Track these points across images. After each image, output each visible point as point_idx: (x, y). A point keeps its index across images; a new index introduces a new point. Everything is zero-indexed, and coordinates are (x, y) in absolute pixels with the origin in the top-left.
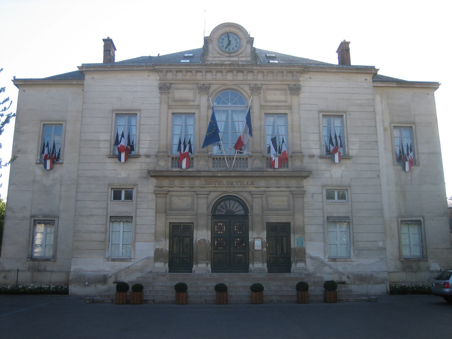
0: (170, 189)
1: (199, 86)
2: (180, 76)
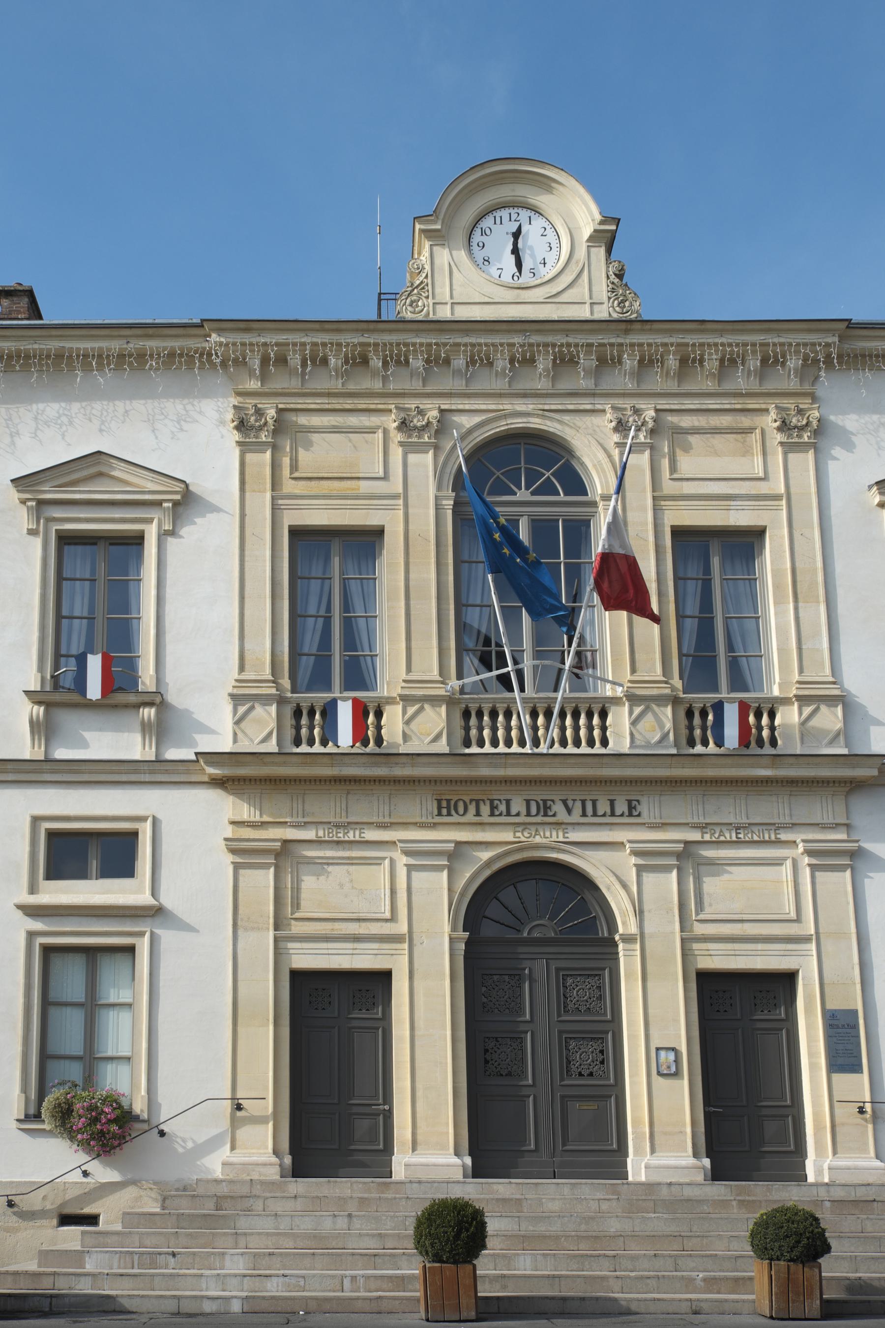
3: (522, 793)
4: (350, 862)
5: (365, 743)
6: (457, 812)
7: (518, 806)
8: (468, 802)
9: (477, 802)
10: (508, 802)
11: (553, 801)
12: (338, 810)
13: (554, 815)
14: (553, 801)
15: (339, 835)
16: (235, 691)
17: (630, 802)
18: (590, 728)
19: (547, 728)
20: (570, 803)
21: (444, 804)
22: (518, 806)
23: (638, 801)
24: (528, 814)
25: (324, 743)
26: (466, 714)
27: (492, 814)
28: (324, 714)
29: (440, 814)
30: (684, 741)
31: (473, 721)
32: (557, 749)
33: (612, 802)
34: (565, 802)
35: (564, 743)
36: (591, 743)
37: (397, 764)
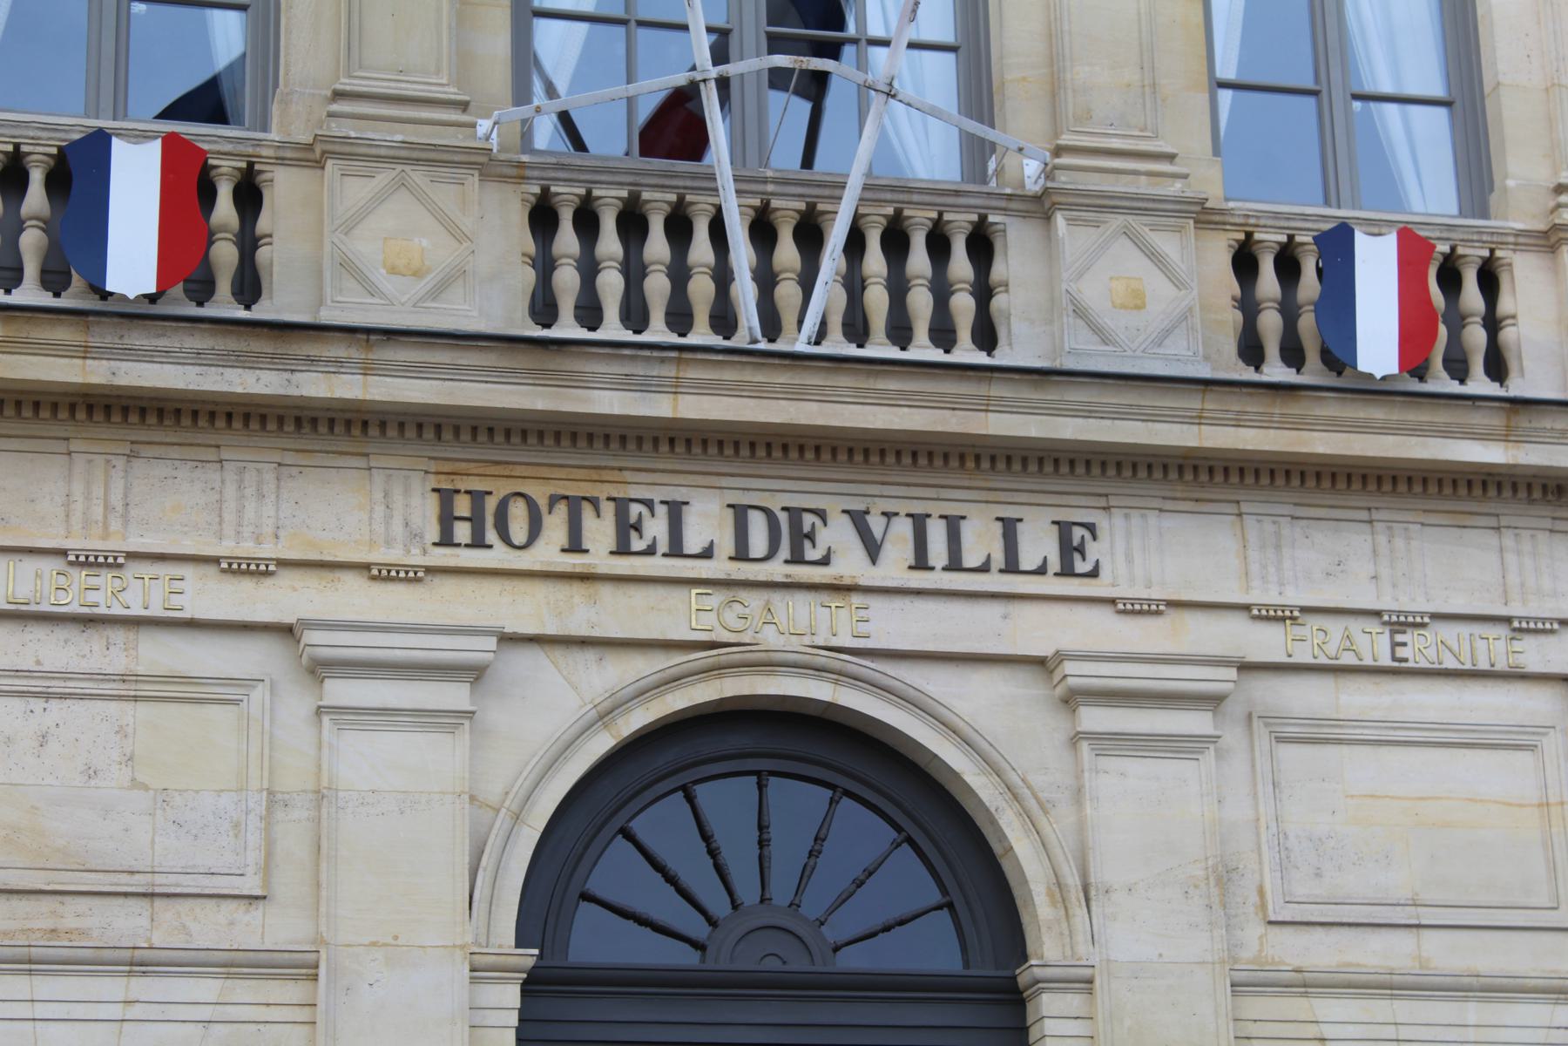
3: (725, 482)
4: (132, 688)
5: (203, 289)
6: (506, 538)
7: (707, 521)
8: (544, 508)
9: (574, 506)
10: (676, 511)
11: (821, 514)
12: (98, 511)
13: (825, 561)
14: (821, 514)
15: (92, 597)
17: (1064, 528)
18: (941, 291)
20: (876, 524)
21: (462, 506)
22: (707, 521)
23: (1091, 528)
24: (741, 554)
25: (54, 279)
26: (543, 218)
27: (623, 550)
28: (59, 180)
29: (446, 540)
30: (1230, 346)
31: (567, 240)
32: (837, 345)
33: (1009, 528)
34: (859, 520)
35: (857, 329)
36: (943, 334)
37: (312, 360)
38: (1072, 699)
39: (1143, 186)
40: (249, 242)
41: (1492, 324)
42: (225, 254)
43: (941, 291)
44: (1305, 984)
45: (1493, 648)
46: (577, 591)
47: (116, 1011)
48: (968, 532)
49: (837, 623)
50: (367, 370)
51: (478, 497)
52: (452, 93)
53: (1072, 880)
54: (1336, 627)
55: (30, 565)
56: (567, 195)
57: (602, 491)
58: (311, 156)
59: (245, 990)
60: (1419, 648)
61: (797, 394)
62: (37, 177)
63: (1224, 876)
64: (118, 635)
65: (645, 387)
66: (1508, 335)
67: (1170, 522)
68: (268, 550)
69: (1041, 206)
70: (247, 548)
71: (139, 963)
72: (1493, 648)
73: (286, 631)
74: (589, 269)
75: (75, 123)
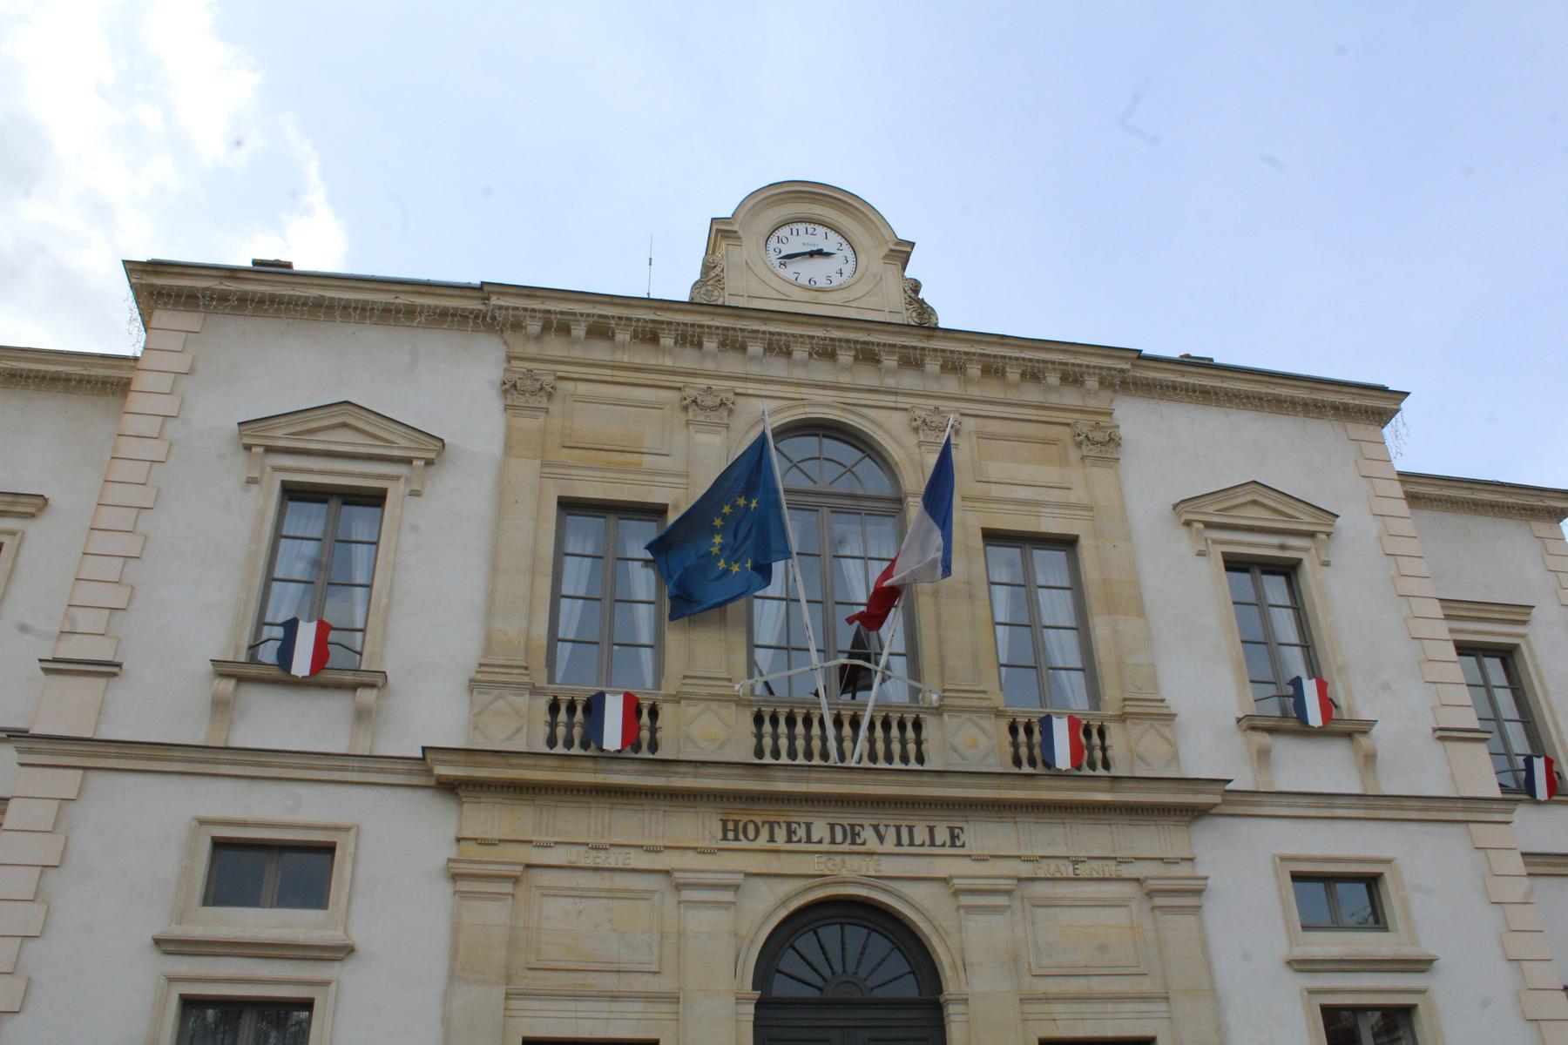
0: (537, 856)
1: (690, 393)
2: (599, 351)
4: (612, 894)
5: (637, 748)
6: (746, 837)
7: (820, 830)
9: (771, 825)
10: (808, 826)
16: (479, 676)
17: (951, 829)
18: (903, 743)
19: (855, 741)
20: (882, 829)
21: (731, 826)
22: (820, 830)
25: (585, 745)
26: (758, 720)
27: (789, 841)
28: (588, 709)
29: (725, 838)
30: (1009, 760)
31: (767, 727)
32: (866, 764)
33: (931, 829)
34: (876, 828)
35: (873, 757)
36: (905, 758)
38: (957, 893)
39: (976, 703)
40: (653, 730)
41: (1104, 749)
42: (645, 735)
43: (903, 743)
44: (1047, 999)
45: (1110, 869)
46: (773, 856)
47: (605, 1015)
48: (916, 831)
49: (869, 867)
50: (696, 776)
51: (736, 822)
52: (725, 675)
53: (959, 961)
54: (1053, 863)
55: (575, 849)
56: (767, 711)
57: (781, 819)
58: (677, 699)
59: (652, 1007)
60: (1083, 870)
61: (851, 782)
62: (579, 709)
63: (1015, 959)
64: (607, 874)
65: (797, 780)
66: (1110, 753)
67: (990, 826)
68: (660, 843)
69: (938, 711)
70: (653, 842)
71: (614, 997)
72: (1110, 869)
73: (667, 873)
74: (775, 737)
75: (593, 690)
